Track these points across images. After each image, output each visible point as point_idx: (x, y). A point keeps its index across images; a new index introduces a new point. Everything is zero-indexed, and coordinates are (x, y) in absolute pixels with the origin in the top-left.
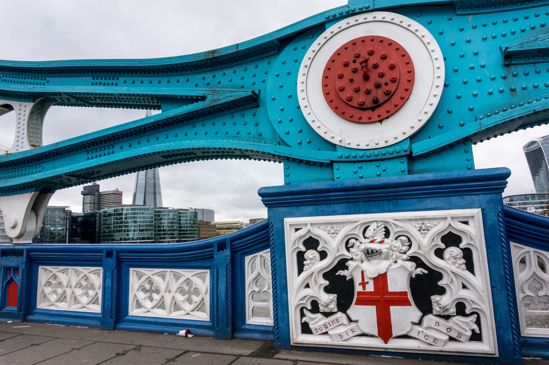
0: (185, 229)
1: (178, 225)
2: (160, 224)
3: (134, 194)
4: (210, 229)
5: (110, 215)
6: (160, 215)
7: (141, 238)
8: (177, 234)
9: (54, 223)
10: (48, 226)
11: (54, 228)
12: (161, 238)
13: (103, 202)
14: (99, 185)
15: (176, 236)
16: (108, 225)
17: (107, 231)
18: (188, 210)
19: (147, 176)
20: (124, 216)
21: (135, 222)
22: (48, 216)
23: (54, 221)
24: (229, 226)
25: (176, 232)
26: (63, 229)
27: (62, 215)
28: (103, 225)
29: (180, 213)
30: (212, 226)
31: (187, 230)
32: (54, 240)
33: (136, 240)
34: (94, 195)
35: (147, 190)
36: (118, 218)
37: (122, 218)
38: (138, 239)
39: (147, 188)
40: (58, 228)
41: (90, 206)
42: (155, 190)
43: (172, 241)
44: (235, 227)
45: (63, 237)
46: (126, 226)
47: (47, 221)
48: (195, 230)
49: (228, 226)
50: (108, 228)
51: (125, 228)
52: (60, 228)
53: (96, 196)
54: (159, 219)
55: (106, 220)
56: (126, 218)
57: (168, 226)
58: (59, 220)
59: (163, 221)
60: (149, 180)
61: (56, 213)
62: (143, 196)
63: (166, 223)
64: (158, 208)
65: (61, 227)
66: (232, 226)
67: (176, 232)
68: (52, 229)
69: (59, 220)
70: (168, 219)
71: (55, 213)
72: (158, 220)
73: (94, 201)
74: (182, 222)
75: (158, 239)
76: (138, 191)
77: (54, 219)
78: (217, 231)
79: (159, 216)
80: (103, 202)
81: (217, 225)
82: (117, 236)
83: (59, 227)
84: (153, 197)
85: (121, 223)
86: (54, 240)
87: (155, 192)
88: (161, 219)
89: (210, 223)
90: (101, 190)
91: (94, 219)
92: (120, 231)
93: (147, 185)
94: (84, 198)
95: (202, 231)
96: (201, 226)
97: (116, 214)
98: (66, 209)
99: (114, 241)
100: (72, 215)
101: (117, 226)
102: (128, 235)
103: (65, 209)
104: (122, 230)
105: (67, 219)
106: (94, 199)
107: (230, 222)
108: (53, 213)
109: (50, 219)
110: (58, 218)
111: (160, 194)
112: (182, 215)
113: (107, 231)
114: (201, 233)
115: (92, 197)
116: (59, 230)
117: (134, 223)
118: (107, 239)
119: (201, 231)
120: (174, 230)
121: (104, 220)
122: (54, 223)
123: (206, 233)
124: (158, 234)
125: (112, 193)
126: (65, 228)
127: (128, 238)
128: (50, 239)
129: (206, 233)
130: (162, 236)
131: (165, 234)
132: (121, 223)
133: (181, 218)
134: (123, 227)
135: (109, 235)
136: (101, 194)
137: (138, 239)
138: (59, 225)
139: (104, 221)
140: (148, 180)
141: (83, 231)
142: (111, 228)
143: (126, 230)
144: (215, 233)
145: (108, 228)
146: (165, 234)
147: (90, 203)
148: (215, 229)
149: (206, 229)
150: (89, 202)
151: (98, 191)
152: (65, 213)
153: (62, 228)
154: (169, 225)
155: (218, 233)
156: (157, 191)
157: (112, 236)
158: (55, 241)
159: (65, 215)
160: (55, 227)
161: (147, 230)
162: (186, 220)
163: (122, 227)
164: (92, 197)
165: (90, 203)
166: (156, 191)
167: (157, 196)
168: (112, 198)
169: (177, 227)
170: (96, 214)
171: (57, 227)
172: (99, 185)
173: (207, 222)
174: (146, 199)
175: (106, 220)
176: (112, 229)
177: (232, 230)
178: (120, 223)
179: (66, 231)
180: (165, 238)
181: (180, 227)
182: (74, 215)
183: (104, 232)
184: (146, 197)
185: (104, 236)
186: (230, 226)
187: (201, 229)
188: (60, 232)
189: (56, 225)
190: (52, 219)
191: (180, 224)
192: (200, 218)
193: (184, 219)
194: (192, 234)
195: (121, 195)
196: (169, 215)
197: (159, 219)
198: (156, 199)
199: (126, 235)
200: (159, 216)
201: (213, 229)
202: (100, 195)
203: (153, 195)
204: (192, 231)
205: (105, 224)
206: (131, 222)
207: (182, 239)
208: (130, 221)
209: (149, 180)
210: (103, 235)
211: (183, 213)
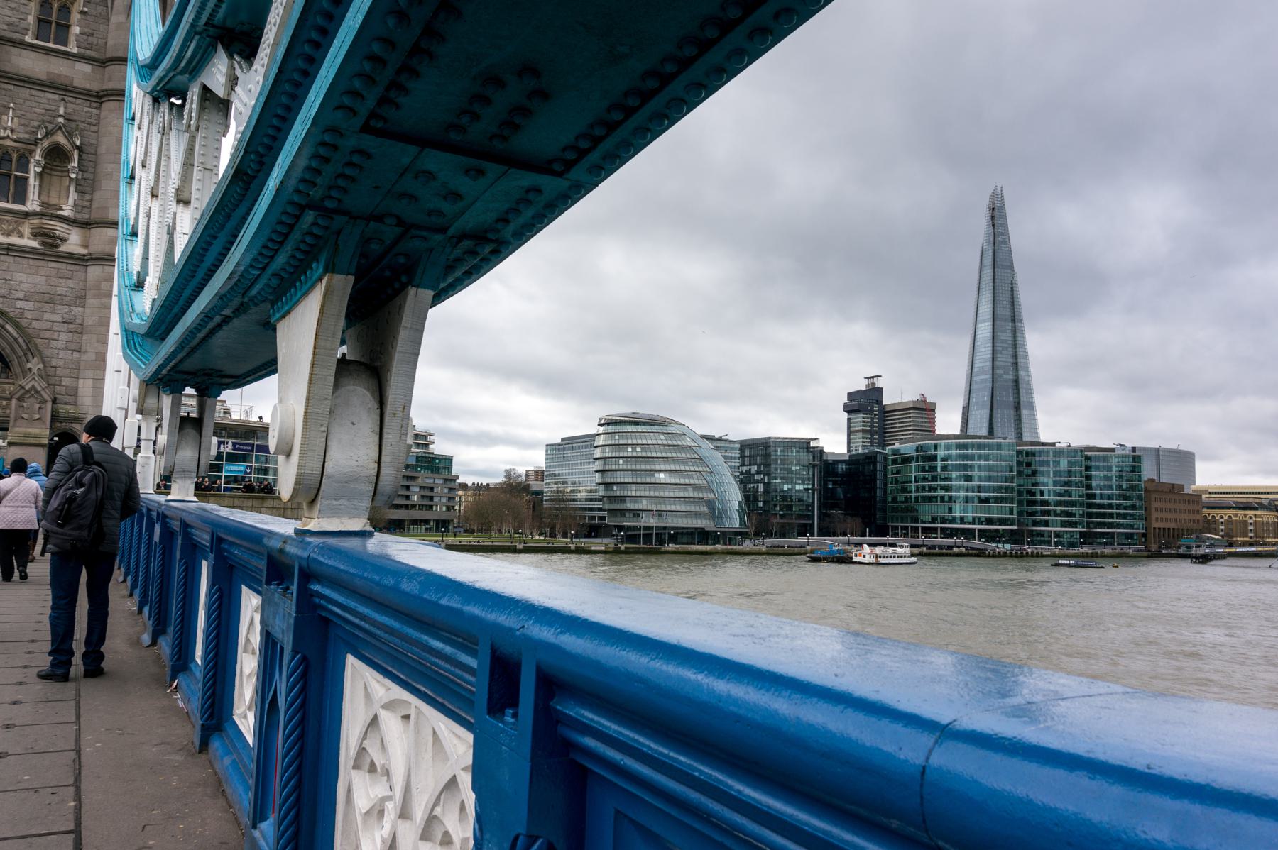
0: (1106, 502)
1: (1083, 491)
2: (1034, 485)
3: (964, 408)
4: (1182, 507)
5: (907, 460)
6: (1033, 463)
7: (983, 519)
8: (1081, 516)
9: (790, 475)
10: (778, 481)
11: (790, 487)
12: (1035, 523)
13: (892, 428)
14: (882, 389)
15: (1077, 519)
16: (902, 483)
17: (901, 497)
18: (1113, 450)
19: (997, 363)
20: (939, 463)
21: (968, 479)
22: (776, 460)
23: (790, 471)
24: (1245, 500)
25: (1078, 510)
26: (808, 489)
27: (806, 458)
28: (891, 483)
29: (1088, 458)
30: (1187, 498)
31: (1110, 506)
32: (789, 512)
33: (970, 524)
34: (871, 412)
35: (997, 398)
36: (927, 468)
37: (934, 468)
38: (977, 521)
39: (997, 393)
40: (797, 487)
41: (863, 438)
42: (1018, 398)
43: (1067, 532)
44: (1266, 503)
45: (807, 506)
46: (947, 489)
47: (776, 469)
48: (1133, 507)
49: (1242, 499)
50: (904, 490)
51: (943, 493)
52: (802, 487)
53: (875, 415)
54: (1030, 472)
55: (898, 472)
56: (944, 468)
57: (1055, 491)
58: (798, 468)
59: (1040, 479)
60: (1002, 372)
61: (792, 452)
62: (986, 412)
63: (1050, 483)
64: (1026, 444)
65: (803, 484)
66: (1257, 501)
67: (1078, 510)
68: (786, 487)
69: (798, 468)
70: (1056, 473)
71: (790, 454)
72: (1027, 476)
73: (872, 426)
74: (1094, 483)
75: (1027, 525)
76: (973, 400)
77: (790, 466)
78: (1205, 511)
79: (1029, 464)
80: (892, 428)
81: (1204, 496)
82: (926, 512)
83: (799, 484)
84: (1012, 417)
85: (934, 479)
86: (789, 512)
87: (1019, 403)
88: (1034, 473)
89: (1181, 487)
90: (887, 400)
91: (872, 467)
92: (930, 499)
93: (996, 385)
94: (849, 420)
95: (1156, 509)
96: (1153, 496)
97: (922, 456)
98: (813, 444)
99: (918, 523)
100: (825, 458)
101: (924, 488)
102: (950, 510)
103: (809, 443)
104: (936, 497)
105: (814, 466)
106: (872, 422)
107: (1262, 487)
108: (786, 454)
109: (782, 466)
110: (796, 465)
111: (1031, 407)
112: (1093, 463)
113: (901, 497)
114: (1155, 515)
115: (868, 418)
116: (799, 491)
117: (966, 481)
118: (902, 517)
119: (1153, 510)
120: (1073, 504)
121: (894, 471)
122: (790, 475)
123: (1169, 515)
124: (1027, 512)
125: (911, 406)
126: (810, 487)
127: (950, 518)
128: (781, 509)
129: (1169, 515)
130: (1038, 518)
131: (1047, 513)
132: (934, 479)
133: (1093, 473)
134: (939, 490)
135: (906, 507)
136: (887, 409)
137: (977, 521)
138: (799, 479)
139: (893, 474)
140: (998, 372)
141: (849, 495)
142: (911, 492)
143: (946, 499)
144: (1197, 517)
145: (904, 490)
146: (1047, 513)
147: (864, 431)
148: (1196, 507)
149: (1169, 506)
150: (861, 428)
151: (879, 402)
152: (811, 454)
153: (806, 487)
154: (1059, 489)
155: (1210, 518)
156: (1023, 399)
157: (914, 510)
158: (792, 515)
159: (811, 458)
160: (791, 483)
161: (999, 500)
162: (1107, 478)
163: (935, 489)
164: (868, 418)
165: (864, 431)
166: (1022, 399)
167: (1024, 412)
168: (911, 420)
169: (1080, 496)
170: (875, 457)
171: (796, 484)
172: (882, 389)
173: (1173, 485)
174: (995, 420)
175: (898, 472)
176: (913, 494)
177: (1258, 512)
178: (930, 479)
179: (813, 494)
180: (1046, 524)
181: (1093, 496)
182: (829, 458)
183: (895, 500)
184: (994, 415)
185: (895, 510)
186: (1250, 500)
187: (1154, 505)
188: (801, 494)
189: (792, 478)
190: (786, 466)
191: (1089, 487)
192: (1148, 472)
193: (1102, 474)
194: (1124, 516)
195: (934, 410)
196: (1057, 463)
197: (1030, 472)
198: (1020, 420)
199: (947, 511)
200: (1029, 464)
201: (1191, 507)
202: (885, 412)
203: (1012, 412)
204: (1125, 508)
205: (897, 482)
206: (959, 478)
207: (1096, 528)
208: (954, 476)
209: (1002, 372)
210: (893, 508)
211: (1098, 459)
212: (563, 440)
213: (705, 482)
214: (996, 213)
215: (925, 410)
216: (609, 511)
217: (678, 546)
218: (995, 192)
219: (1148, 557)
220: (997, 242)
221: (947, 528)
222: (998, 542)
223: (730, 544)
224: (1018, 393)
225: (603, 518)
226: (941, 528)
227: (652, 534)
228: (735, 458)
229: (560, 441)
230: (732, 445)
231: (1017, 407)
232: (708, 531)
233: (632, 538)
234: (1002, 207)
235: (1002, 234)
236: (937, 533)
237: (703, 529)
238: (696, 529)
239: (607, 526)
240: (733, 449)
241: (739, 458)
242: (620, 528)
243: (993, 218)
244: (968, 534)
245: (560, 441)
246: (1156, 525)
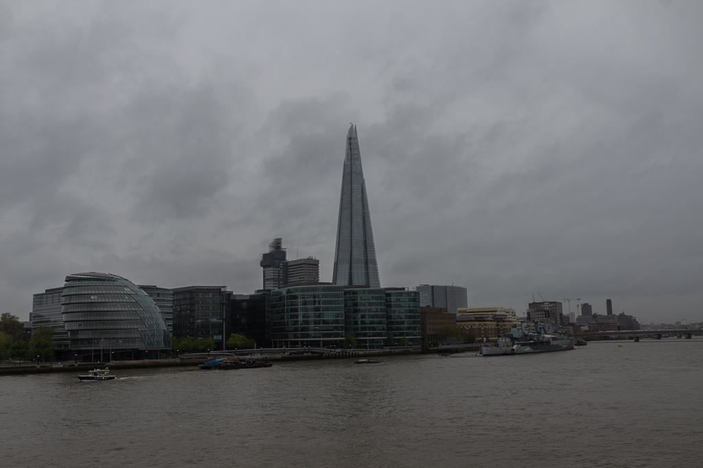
42: (367, 257)
73: (279, 276)
78: (457, 323)
89: (446, 310)
90: (289, 258)
94: (264, 271)
106: (279, 273)
136: (289, 265)
167: (370, 266)
202: (287, 266)
212: (47, 291)
213: (139, 318)
214: (352, 141)
215: (313, 265)
216: (72, 340)
217: (117, 362)
218: (352, 128)
219: (422, 353)
220: (353, 158)
221: (304, 341)
222: (332, 348)
223: (157, 358)
224: (367, 254)
225: (66, 345)
226: (301, 341)
227: (91, 356)
228: (169, 301)
229: (44, 292)
230: (168, 292)
231: (366, 263)
232: (141, 351)
233: (87, 358)
234: (356, 138)
235: (355, 154)
236: (298, 344)
237: (137, 349)
238: (132, 349)
239: (71, 351)
240: (168, 295)
241: (173, 301)
242: (79, 352)
243: (350, 144)
244: (317, 344)
245: (44, 292)
246: (429, 333)
